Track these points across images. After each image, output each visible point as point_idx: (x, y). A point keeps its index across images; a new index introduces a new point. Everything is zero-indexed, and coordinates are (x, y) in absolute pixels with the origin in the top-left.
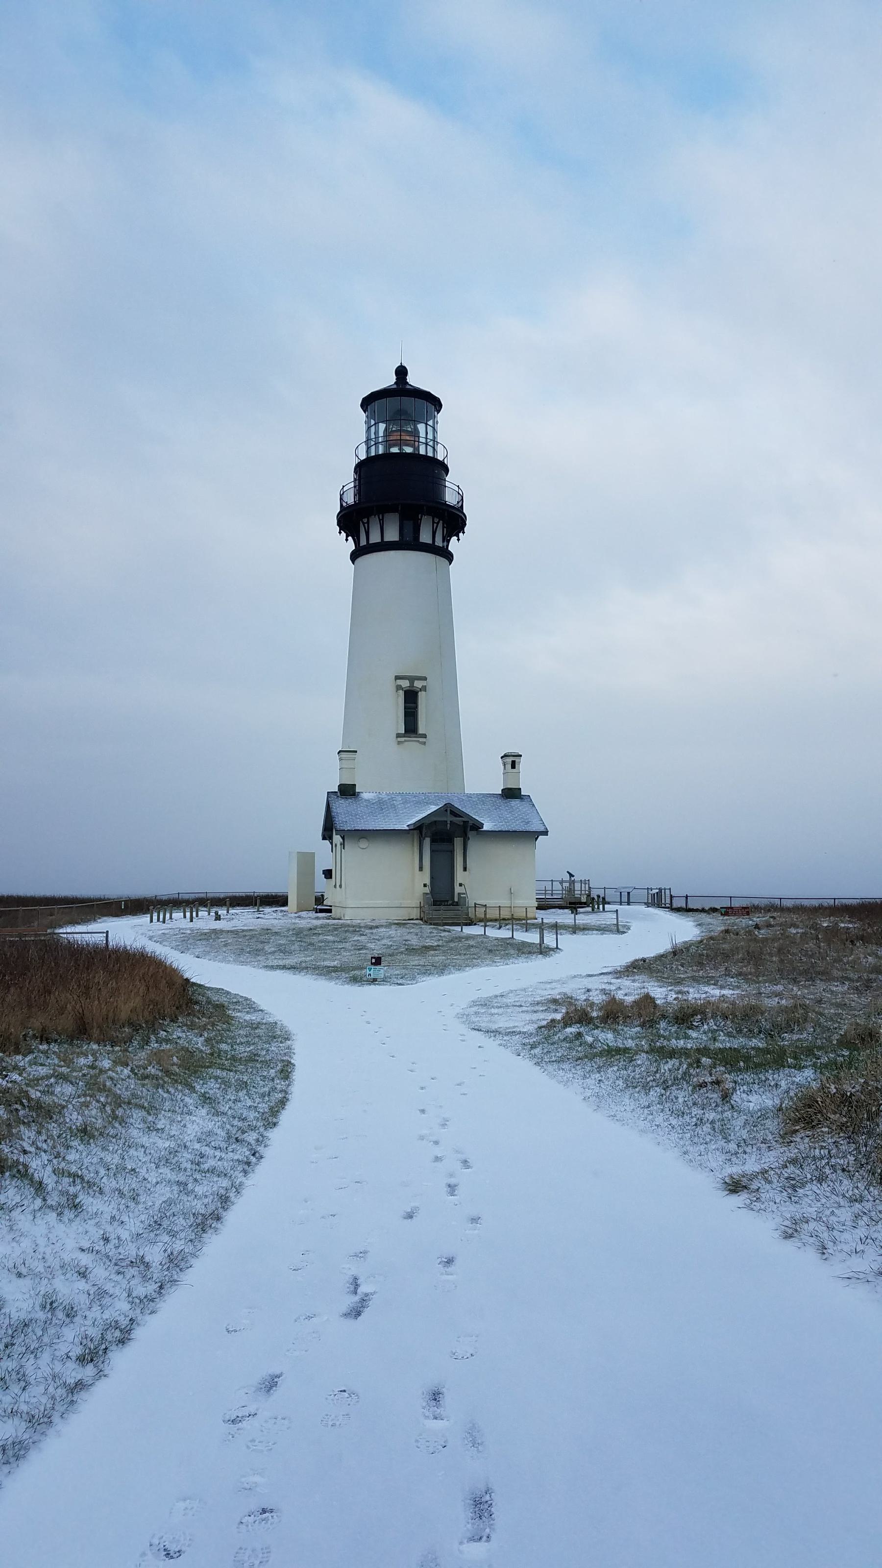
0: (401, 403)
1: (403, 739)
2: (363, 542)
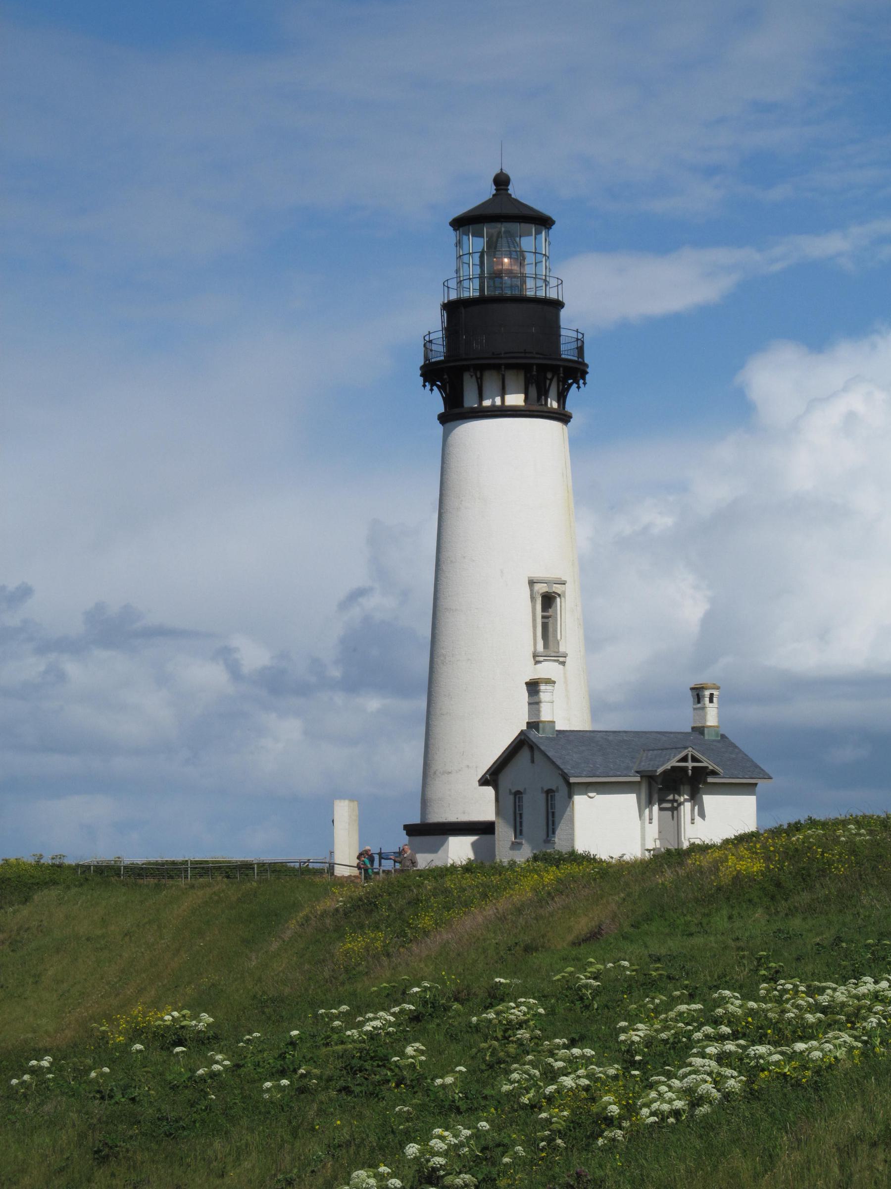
1: (541, 659)
2: (470, 401)
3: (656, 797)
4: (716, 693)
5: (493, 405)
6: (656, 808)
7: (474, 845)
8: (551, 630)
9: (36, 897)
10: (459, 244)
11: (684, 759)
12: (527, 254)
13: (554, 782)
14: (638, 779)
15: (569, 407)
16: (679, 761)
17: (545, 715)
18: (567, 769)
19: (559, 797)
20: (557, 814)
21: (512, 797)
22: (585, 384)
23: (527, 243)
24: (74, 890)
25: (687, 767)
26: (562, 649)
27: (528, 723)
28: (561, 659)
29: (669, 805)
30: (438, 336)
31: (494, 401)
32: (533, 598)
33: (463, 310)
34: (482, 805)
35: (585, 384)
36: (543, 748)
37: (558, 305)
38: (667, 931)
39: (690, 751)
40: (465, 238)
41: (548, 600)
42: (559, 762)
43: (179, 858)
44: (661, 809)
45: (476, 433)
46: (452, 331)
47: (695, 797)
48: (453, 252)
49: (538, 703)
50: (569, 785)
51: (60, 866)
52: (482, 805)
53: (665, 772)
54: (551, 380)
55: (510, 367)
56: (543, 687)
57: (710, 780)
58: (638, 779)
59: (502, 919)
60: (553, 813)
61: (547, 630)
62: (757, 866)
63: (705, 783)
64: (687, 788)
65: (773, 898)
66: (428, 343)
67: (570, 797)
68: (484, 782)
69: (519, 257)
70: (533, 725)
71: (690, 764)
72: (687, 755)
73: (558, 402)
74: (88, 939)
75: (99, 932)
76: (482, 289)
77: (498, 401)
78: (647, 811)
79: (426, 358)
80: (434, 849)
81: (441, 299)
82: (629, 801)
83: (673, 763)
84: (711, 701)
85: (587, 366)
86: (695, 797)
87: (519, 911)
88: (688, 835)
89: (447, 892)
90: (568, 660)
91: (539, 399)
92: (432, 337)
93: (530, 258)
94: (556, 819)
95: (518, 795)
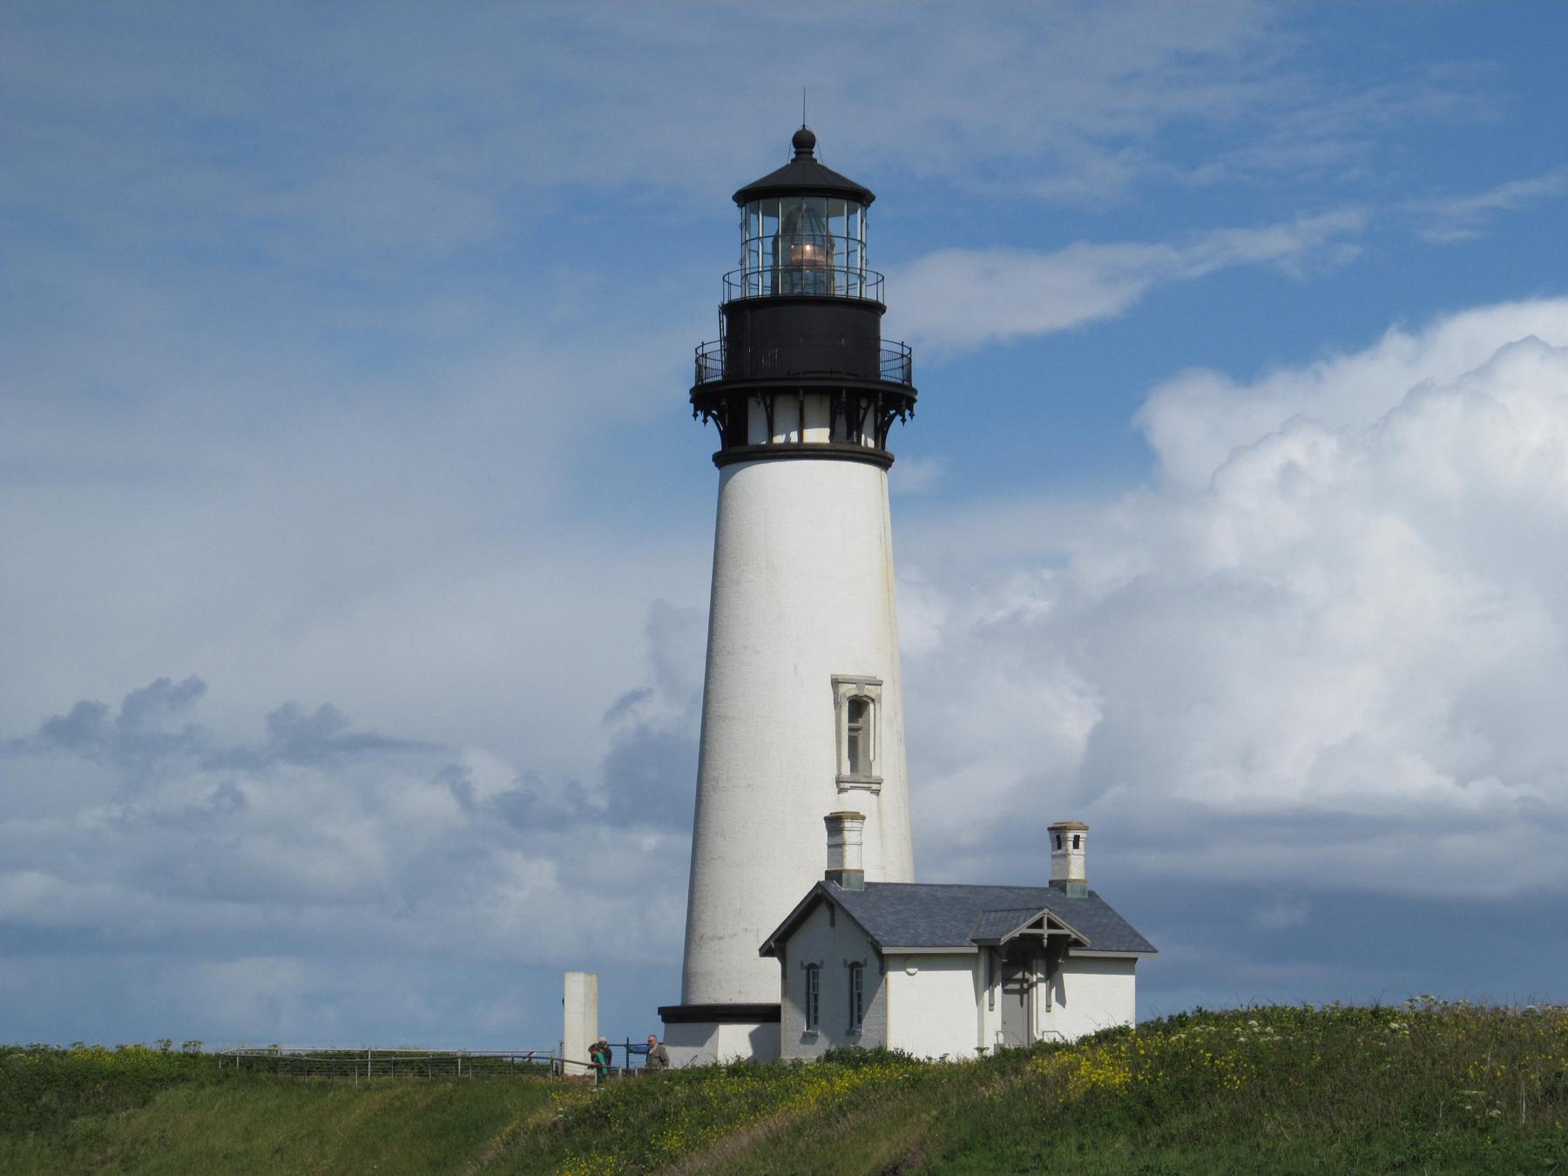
0: (803, 189)
1: (847, 785)
2: (757, 437)
3: (998, 975)
4: (1082, 835)
5: (788, 442)
6: (998, 990)
7: (753, 1037)
8: (861, 746)
9: (158, 1098)
10: (745, 225)
11: (1038, 924)
12: (836, 240)
13: (862, 953)
14: (975, 950)
15: (891, 446)
16: (1031, 927)
17: (851, 862)
18: (879, 935)
19: (868, 972)
20: (863, 997)
21: (804, 972)
22: (912, 415)
23: (837, 225)
24: (209, 1090)
25: (1039, 937)
26: (876, 772)
27: (827, 873)
28: (875, 787)
29: (1017, 986)
30: (715, 348)
31: (788, 437)
32: (837, 704)
33: (748, 313)
34: (764, 982)
35: (912, 415)
36: (846, 906)
37: (877, 309)
38: (991, 1165)
39: (1045, 913)
40: (753, 217)
41: (858, 707)
42: (867, 926)
43: (356, 1047)
44: (1005, 992)
45: (765, 482)
46: (733, 342)
47: (1052, 976)
48: (736, 236)
49: (841, 845)
50: (882, 957)
51: (194, 1056)
52: (764, 982)
53: (1012, 941)
54: (866, 410)
55: (811, 391)
56: (847, 824)
57: (1072, 953)
58: (975, 950)
59: (776, 1141)
60: (859, 995)
61: (856, 747)
62: (1120, 1077)
63: (1067, 957)
64: (1041, 963)
65: (1141, 1122)
66: (701, 359)
67: (882, 972)
68: (766, 951)
69: (826, 244)
70: (834, 875)
71: (1046, 931)
72: (1041, 919)
73: (876, 440)
74: (225, 1157)
75: (241, 1147)
76: (774, 285)
77: (794, 437)
78: (987, 994)
79: (699, 376)
80: (700, 1042)
81: (719, 298)
82: (962, 980)
83: (1023, 929)
84: (1076, 846)
85: (915, 392)
86: (1052, 976)
87: (799, 1131)
88: (1042, 1027)
89: (704, 1101)
90: (884, 788)
91: (849, 435)
92: (707, 349)
93: (840, 245)
94: (864, 1003)
95: (812, 969)
